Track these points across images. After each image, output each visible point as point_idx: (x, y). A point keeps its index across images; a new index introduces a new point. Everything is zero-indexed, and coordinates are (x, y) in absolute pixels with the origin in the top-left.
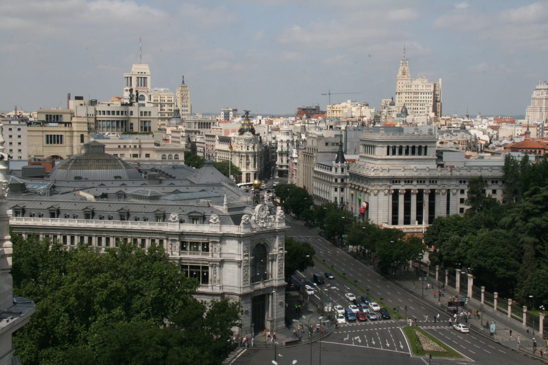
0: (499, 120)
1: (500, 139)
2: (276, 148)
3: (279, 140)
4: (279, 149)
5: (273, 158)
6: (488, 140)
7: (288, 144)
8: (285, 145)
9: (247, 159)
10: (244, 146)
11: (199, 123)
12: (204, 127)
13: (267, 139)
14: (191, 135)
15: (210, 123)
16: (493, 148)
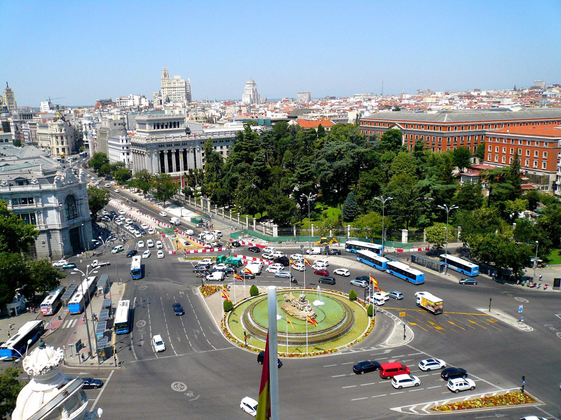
0: (225, 103)
1: (226, 115)
2: (82, 129)
3: (83, 124)
4: (84, 130)
5: (81, 136)
6: (220, 115)
7: (90, 126)
8: (88, 127)
9: (62, 138)
10: (57, 130)
11: (23, 115)
12: (28, 118)
13: (74, 123)
14: (18, 124)
15: (31, 115)
16: (222, 121)
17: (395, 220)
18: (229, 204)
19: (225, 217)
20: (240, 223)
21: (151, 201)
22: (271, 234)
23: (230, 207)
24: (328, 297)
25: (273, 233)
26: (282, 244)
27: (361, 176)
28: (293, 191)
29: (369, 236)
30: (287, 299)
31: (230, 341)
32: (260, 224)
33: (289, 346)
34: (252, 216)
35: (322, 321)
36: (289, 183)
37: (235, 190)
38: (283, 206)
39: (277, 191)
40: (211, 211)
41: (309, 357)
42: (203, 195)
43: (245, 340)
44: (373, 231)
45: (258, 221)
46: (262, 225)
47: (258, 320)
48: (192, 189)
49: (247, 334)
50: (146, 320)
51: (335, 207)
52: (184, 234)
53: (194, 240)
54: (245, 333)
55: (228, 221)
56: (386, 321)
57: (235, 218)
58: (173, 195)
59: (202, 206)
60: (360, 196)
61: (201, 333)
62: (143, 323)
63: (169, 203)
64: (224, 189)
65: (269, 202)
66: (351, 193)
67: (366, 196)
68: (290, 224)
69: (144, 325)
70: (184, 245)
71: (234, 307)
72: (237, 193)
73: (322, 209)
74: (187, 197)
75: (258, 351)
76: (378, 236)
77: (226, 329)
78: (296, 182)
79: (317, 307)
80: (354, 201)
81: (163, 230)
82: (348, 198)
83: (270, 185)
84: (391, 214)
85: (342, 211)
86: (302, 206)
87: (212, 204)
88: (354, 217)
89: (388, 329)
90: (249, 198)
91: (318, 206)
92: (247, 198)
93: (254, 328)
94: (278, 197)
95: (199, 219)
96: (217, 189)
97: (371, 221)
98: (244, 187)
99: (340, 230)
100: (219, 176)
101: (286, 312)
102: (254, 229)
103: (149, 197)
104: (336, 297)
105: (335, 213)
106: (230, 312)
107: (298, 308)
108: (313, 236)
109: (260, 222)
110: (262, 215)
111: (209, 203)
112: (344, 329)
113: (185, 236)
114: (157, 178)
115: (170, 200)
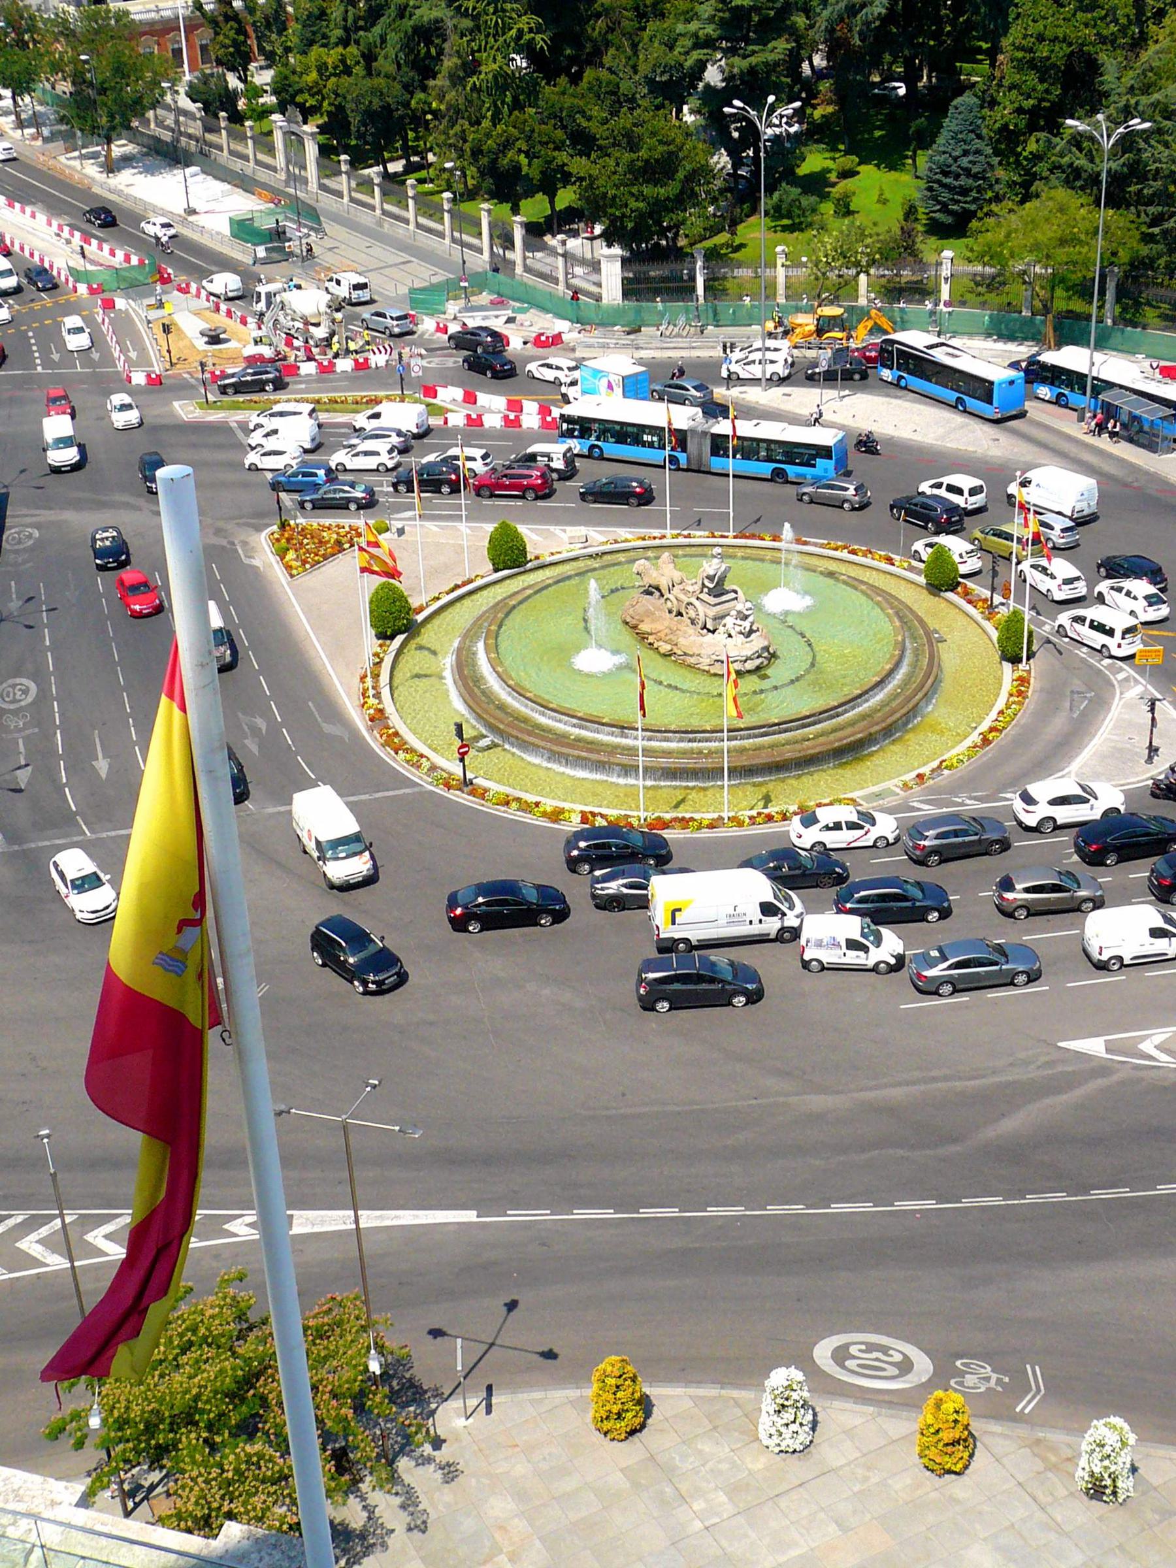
17: (1156, 230)
18: (407, 152)
19: (384, 212)
20: (454, 240)
21: (46, 140)
22: (594, 289)
23: (410, 169)
24: (831, 574)
25: (599, 285)
26: (639, 338)
27: (1018, 16)
28: (701, 85)
29: (1038, 304)
30: (647, 581)
31: (398, 762)
32: (544, 247)
33: (649, 783)
34: (507, 207)
35: (798, 679)
36: (678, 50)
37: (431, 83)
38: (647, 161)
39: (625, 87)
40: (323, 187)
41: (736, 832)
42: (282, 108)
43: (462, 760)
44: (1056, 281)
45: (535, 231)
46: (553, 252)
47: (520, 676)
48: (233, 81)
49: (468, 733)
50: (38, 676)
51: (892, 167)
52: (198, 295)
53: (244, 322)
54: (459, 729)
55: (400, 230)
56: (1077, 684)
57: (430, 217)
58: (144, 109)
59: (280, 160)
60: (1004, 113)
61: (274, 728)
62: (26, 692)
63: (131, 149)
64: (380, 82)
65: (584, 142)
66: (966, 99)
67: (1034, 113)
68: (682, 242)
69: (30, 699)
70: (201, 343)
71: (420, 618)
72: (441, 98)
73: (833, 177)
74: (213, 121)
75: (514, 805)
76: (1077, 306)
77: (381, 711)
78: (709, 43)
79: (784, 618)
80: (979, 137)
81: (105, 277)
82: (950, 124)
83: (594, 58)
84: (1142, 201)
85: (922, 184)
86: (737, 163)
87: (325, 151)
88: (972, 215)
89: (1083, 714)
90: (496, 120)
91: (814, 161)
92: (486, 123)
93: (502, 707)
94: (625, 120)
95: (268, 224)
96: (346, 80)
97: (1047, 233)
98: (472, 68)
99: (907, 275)
100: (357, 18)
101: (642, 637)
102: (519, 270)
103: (36, 121)
104: (866, 576)
105: (887, 195)
106: (400, 638)
107: (693, 622)
108: (781, 300)
109: (548, 238)
110: (552, 202)
111: (311, 150)
112: (893, 712)
113: (203, 302)
114: (66, 31)
115: (134, 136)
